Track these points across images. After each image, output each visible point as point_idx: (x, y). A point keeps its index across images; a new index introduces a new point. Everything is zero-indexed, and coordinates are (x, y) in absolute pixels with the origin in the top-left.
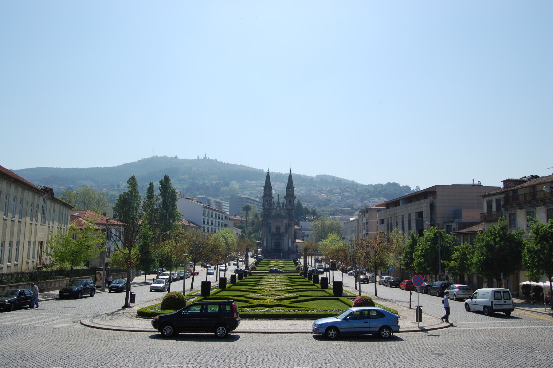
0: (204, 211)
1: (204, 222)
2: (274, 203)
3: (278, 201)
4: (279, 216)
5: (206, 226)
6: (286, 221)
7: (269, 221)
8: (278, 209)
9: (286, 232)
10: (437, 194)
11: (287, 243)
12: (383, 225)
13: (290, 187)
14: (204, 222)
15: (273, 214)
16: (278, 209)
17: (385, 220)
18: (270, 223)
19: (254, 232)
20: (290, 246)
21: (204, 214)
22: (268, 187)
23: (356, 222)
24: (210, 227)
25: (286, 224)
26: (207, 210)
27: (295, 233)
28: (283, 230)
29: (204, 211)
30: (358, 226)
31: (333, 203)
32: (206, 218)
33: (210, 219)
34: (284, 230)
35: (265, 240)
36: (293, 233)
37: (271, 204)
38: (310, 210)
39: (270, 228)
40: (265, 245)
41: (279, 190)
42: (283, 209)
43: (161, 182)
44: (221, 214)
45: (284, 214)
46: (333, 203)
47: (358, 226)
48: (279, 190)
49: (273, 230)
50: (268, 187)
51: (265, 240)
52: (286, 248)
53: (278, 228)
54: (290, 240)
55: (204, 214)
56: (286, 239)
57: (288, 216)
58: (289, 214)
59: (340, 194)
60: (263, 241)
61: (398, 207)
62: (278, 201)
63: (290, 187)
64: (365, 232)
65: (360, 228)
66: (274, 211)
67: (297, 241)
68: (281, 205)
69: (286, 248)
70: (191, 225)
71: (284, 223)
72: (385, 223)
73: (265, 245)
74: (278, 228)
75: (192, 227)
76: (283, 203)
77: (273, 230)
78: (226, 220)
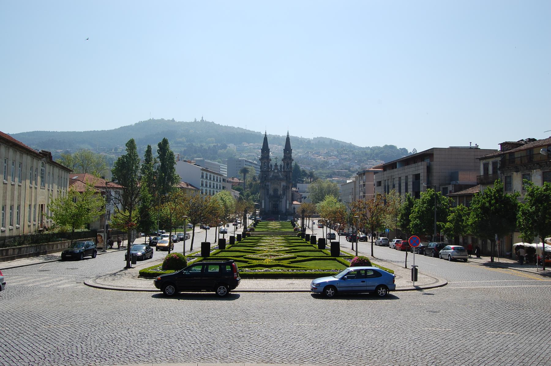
0: (203, 173)
1: (202, 185)
2: (271, 166)
3: (276, 164)
4: (276, 178)
5: (204, 189)
6: (283, 183)
7: (267, 183)
8: (276, 171)
9: (284, 194)
10: (435, 156)
11: (284, 205)
12: (380, 187)
13: (288, 149)
14: (202, 185)
15: (271, 176)
16: (276, 171)
17: (382, 182)
18: (268, 185)
19: (252, 194)
20: (288, 207)
21: (202, 177)
22: (265, 149)
23: (353, 184)
24: (208, 189)
25: (284, 186)
26: (205, 173)
27: (293, 195)
28: (280, 192)
29: (203, 173)
30: (355, 187)
31: (330, 166)
32: (205, 181)
33: (208, 182)
35: (263, 202)
36: (290, 195)
37: (269, 167)
38: (308, 172)
39: (268, 190)
40: (263, 207)
41: (276, 152)
42: (281, 171)
43: (159, 145)
44: (219, 177)
45: (281, 177)
46: (330, 166)
47: (355, 187)
48: (276, 152)
49: (271, 192)
50: (265, 149)
51: (263, 202)
52: (284, 210)
53: (276, 190)
54: (288, 202)
55: (202, 177)
57: (285, 178)
58: (286, 176)
59: (337, 157)
60: (261, 203)
61: (395, 170)
62: (276, 164)
63: (288, 149)
64: (362, 194)
65: (357, 190)
67: (295, 202)
68: (279, 167)
69: (284, 210)
70: (190, 187)
71: (282, 185)
72: (382, 184)
73: (263, 207)
74: (276, 190)
75: (190, 189)
76: (281, 166)
78: (224, 183)
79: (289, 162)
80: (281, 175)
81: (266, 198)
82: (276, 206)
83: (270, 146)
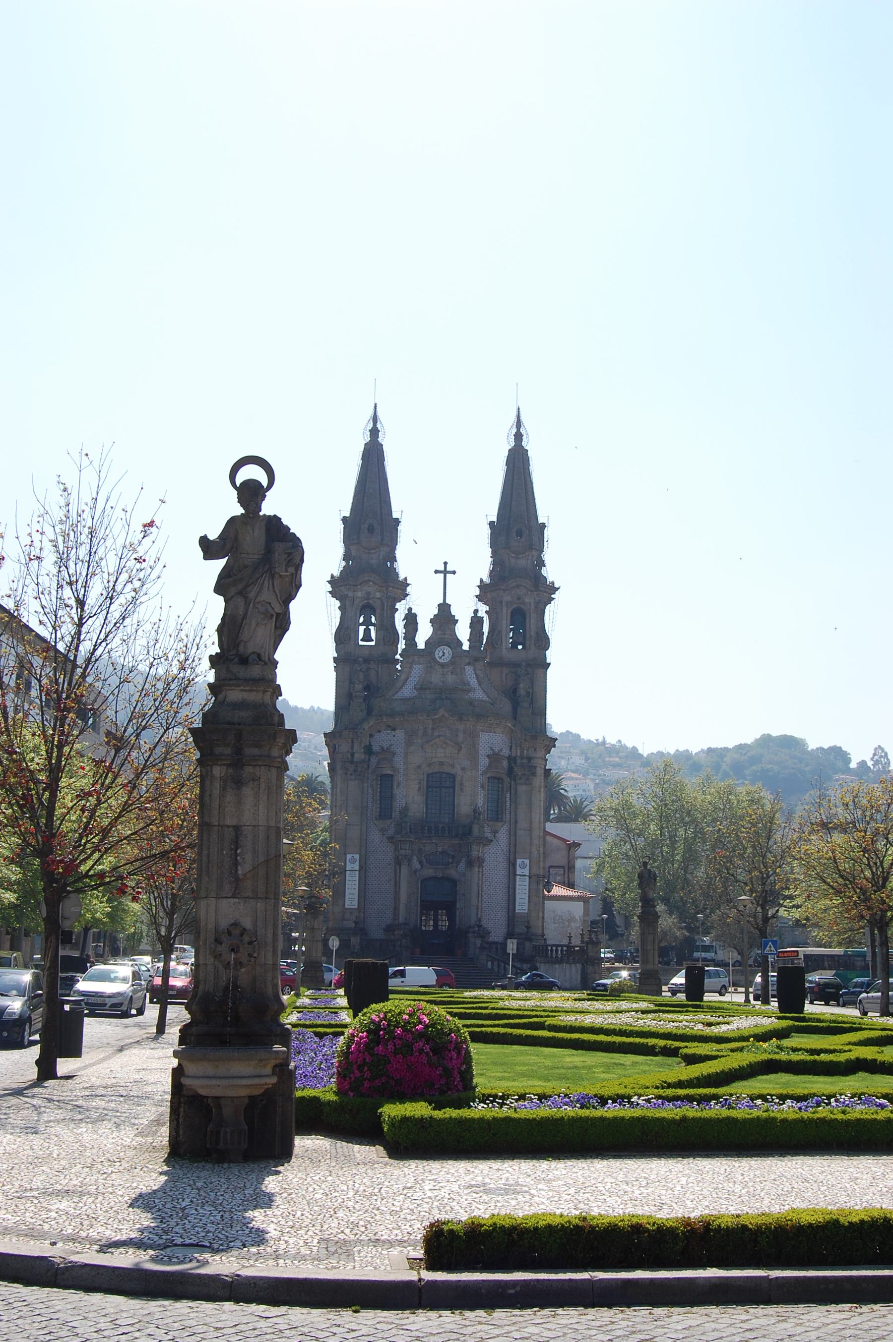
2: (411, 620)
3: (444, 608)
6: (492, 740)
7: (382, 739)
8: (444, 654)
9: (497, 815)
15: (407, 691)
18: (387, 753)
20: (522, 904)
25: (494, 757)
28: (472, 797)
34: (480, 801)
35: (353, 865)
39: (386, 782)
45: (479, 694)
49: (410, 796)
53: (440, 784)
54: (523, 869)
56: (494, 857)
57: (506, 706)
62: (444, 608)
66: (417, 670)
68: (463, 632)
71: (483, 751)
73: (351, 898)
74: (440, 784)
76: (476, 622)
77: (410, 796)
79: (529, 600)
80: (476, 686)
81: (375, 837)
82: (442, 897)
83: (401, 503)
